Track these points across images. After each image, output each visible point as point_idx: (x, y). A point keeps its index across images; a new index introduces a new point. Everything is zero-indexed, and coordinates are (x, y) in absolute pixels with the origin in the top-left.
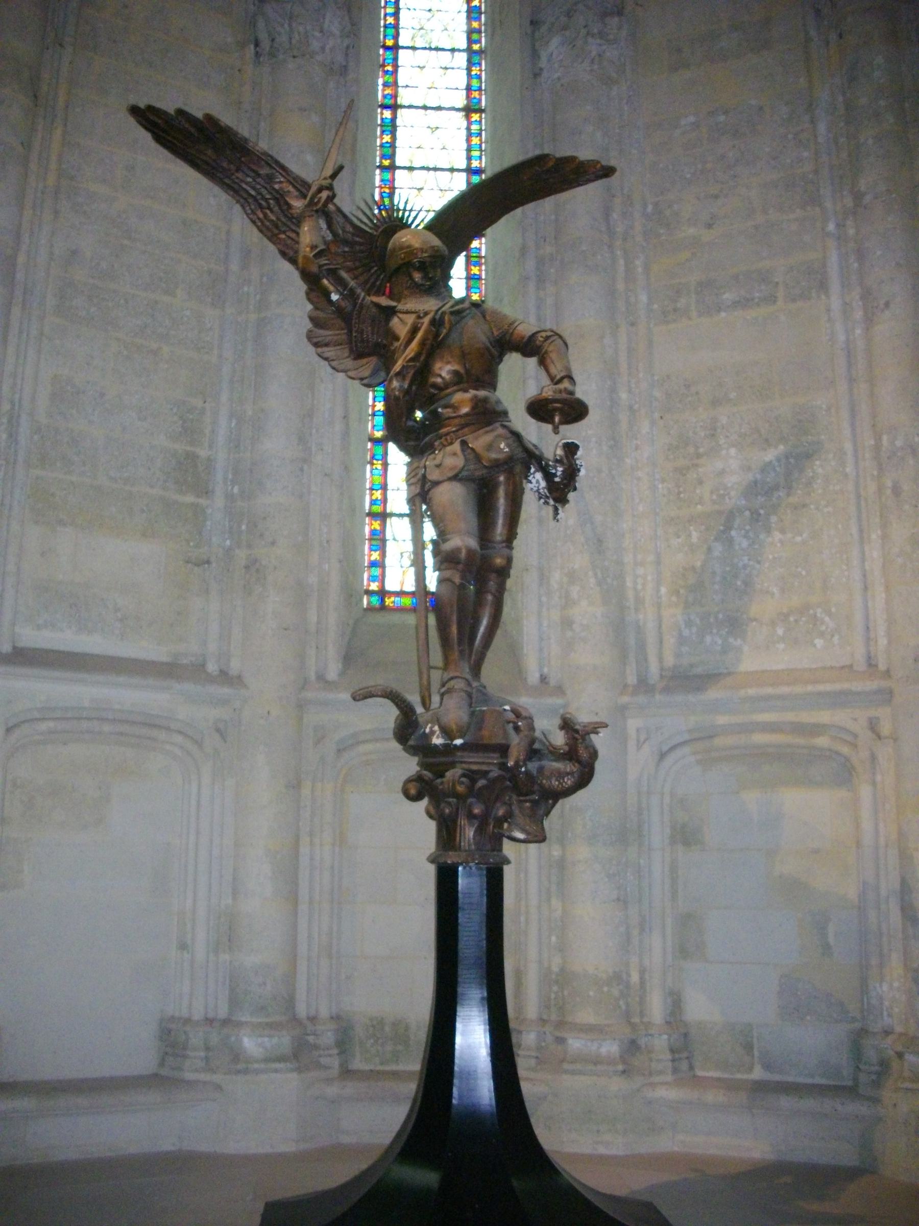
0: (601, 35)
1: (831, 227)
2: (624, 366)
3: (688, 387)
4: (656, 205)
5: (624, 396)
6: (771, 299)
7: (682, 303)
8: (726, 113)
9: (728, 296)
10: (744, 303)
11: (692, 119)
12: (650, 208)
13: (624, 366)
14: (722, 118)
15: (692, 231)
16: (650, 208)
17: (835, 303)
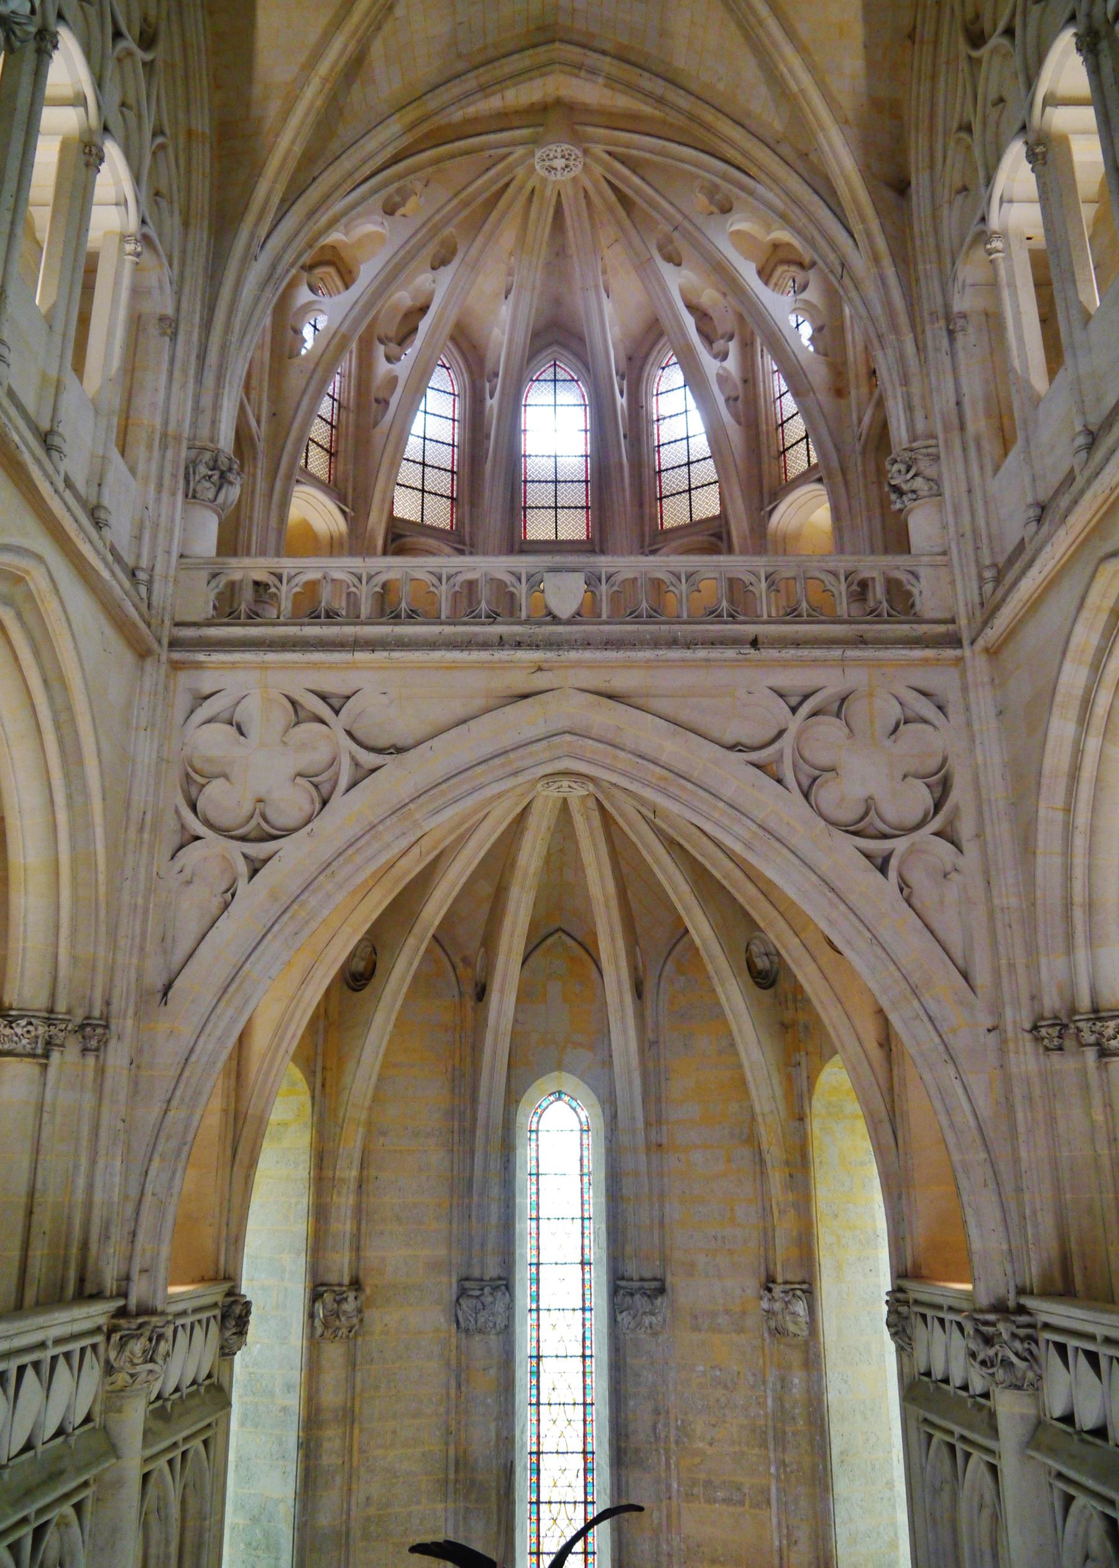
0: (652, 1314)
1: (773, 1470)
2: (664, 1528)
3: (699, 1546)
4: (683, 1421)
5: (665, 1547)
6: (742, 1503)
7: (695, 1490)
8: (720, 1370)
9: (720, 1494)
10: (727, 1501)
11: (701, 1368)
12: (679, 1423)
13: (664, 1528)
14: (718, 1373)
15: (701, 1445)
16: (679, 1423)
17: (774, 1520)
